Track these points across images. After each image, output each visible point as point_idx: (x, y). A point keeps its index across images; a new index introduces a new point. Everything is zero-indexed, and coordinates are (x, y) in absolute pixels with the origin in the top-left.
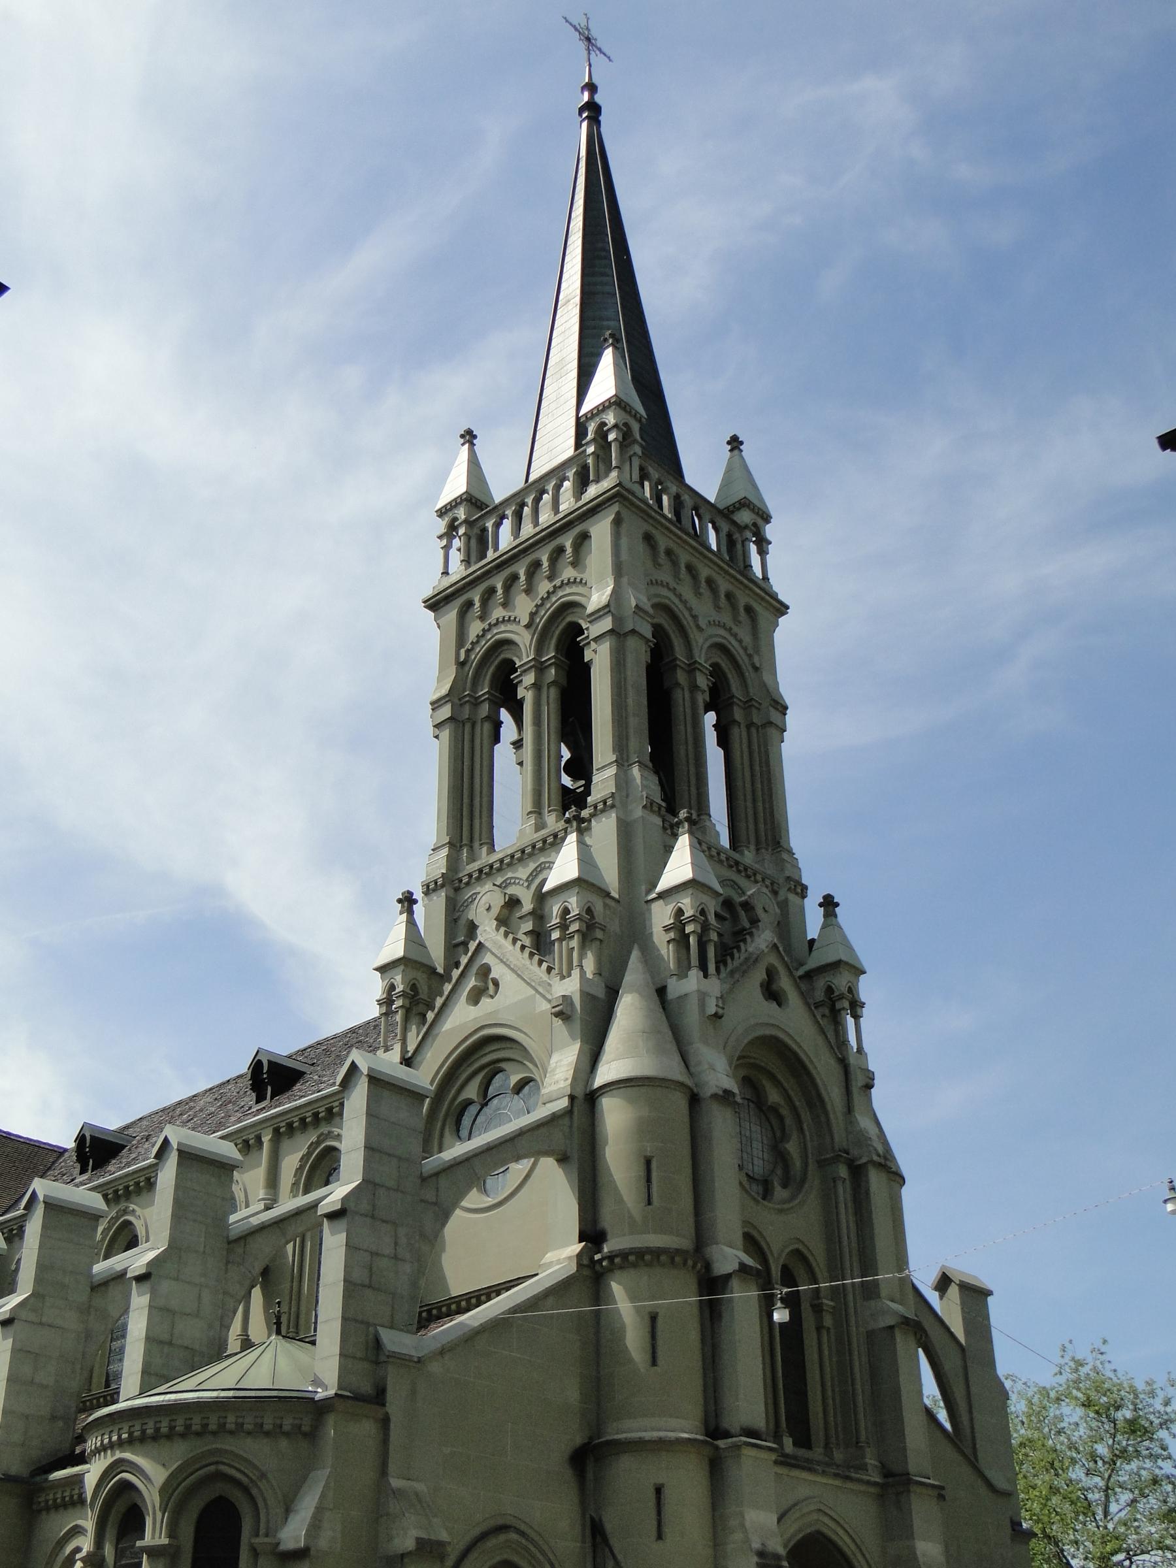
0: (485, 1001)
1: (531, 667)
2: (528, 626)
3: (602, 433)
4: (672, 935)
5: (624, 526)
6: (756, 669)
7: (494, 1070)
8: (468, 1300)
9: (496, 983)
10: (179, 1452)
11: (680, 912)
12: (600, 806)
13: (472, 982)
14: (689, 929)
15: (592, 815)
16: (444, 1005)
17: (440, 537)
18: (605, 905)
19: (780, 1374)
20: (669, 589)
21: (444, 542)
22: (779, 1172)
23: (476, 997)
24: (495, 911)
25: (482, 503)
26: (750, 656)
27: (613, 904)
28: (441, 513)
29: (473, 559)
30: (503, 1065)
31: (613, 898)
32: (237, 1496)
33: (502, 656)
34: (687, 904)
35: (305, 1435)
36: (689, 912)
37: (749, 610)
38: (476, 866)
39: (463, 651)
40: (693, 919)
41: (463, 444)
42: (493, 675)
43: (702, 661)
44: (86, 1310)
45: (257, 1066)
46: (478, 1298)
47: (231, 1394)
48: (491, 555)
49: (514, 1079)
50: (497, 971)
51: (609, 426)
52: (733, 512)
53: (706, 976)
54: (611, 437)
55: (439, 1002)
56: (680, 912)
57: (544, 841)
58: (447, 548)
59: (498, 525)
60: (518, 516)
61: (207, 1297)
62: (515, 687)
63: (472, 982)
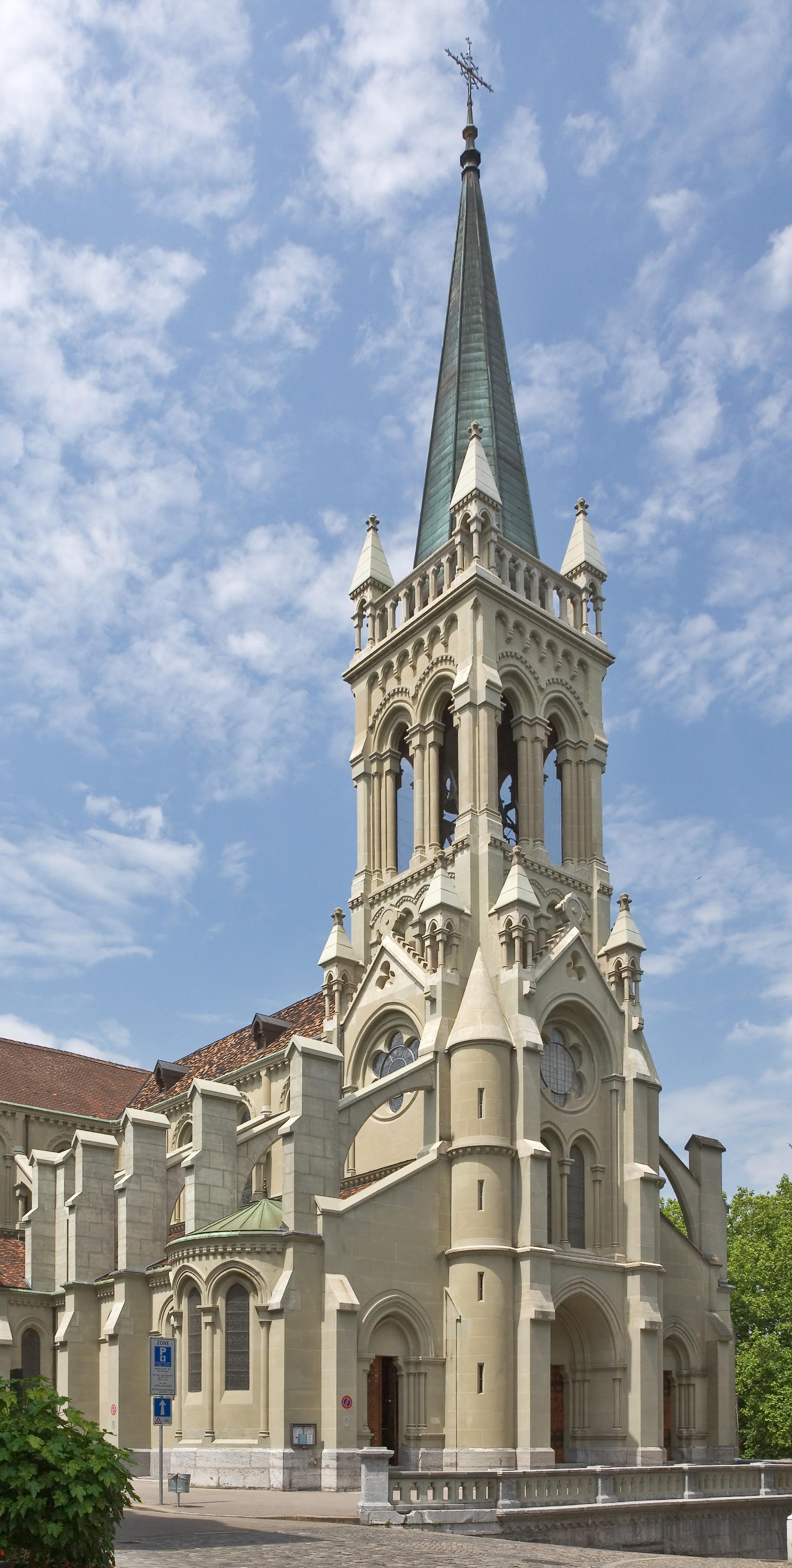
0: (387, 985)
1: (417, 732)
2: (415, 697)
3: (466, 525)
4: (503, 939)
5: (481, 610)
6: (585, 714)
7: (394, 1033)
8: (385, 1172)
9: (393, 975)
10: (215, 1262)
11: (509, 923)
12: (460, 845)
13: (379, 973)
14: (515, 934)
15: (454, 853)
16: (362, 989)
17: (353, 618)
18: (461, 920)
19: (566, 1208)
20: (517, 658)
21: (356, 622)
22: (576, 1087)
23: (382, 982)
24: (392, 924)
25: (384, 585)
26: (581, 704)
27: (466, 918)
28: (354, 595)
29: (377, 637)
30: (399, 1029)
31: (467, 915)
32: (246, 1284)
33: (399, 720)
34: (515, 916)
35: (279, 1253)
36: (515, 923)
37: (582, 664)
38: (383, 887)
39: (371, 718)
40: (518, 928)
41: (368, 530)
42: (393, 736)
43: (542, 717)
44: (165, 1182)
45: (256, 1025)
46: (385, 1172)
47: (237, 1233)
48: (390, 635)
49: (406, 1037)
50: (393, 967)
51: (472, 517)
52: (571, 578)
53: (525, 967)
54: (473, 528)
55: (360, 986)
56: (509, 923)
57: (426, 869)
58: (359, 626)
59: (394, 606)
60: (410, 596)
61: (227, 1176)
62: (407, 746)
63: (379, 973)
